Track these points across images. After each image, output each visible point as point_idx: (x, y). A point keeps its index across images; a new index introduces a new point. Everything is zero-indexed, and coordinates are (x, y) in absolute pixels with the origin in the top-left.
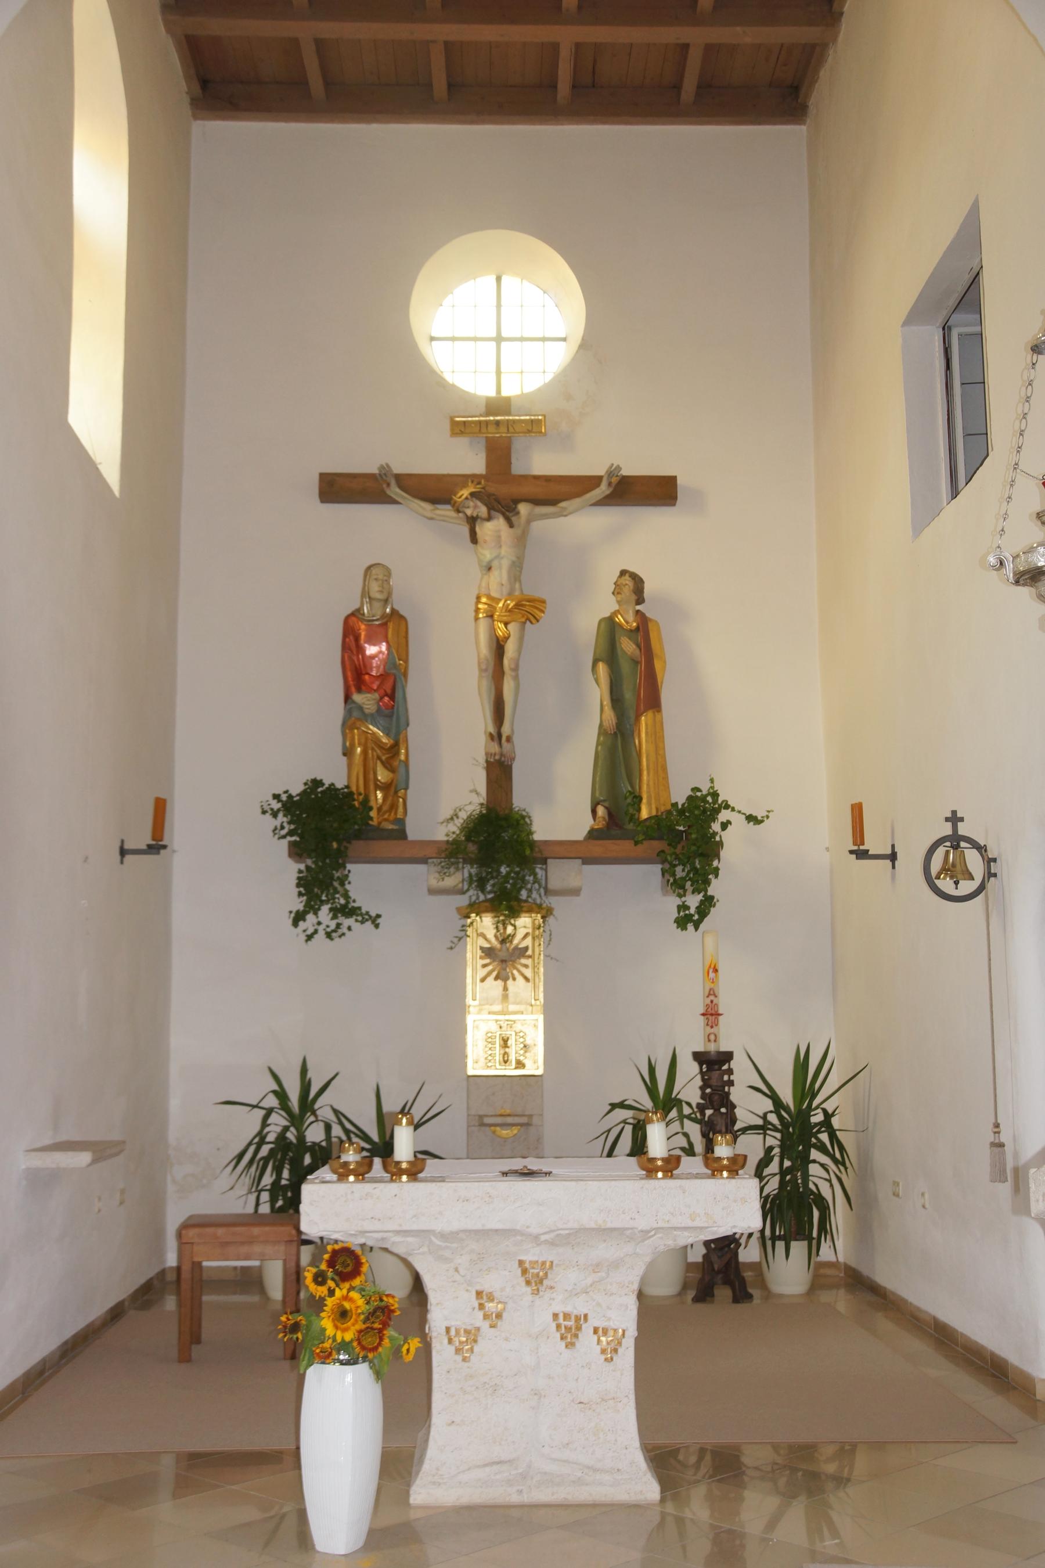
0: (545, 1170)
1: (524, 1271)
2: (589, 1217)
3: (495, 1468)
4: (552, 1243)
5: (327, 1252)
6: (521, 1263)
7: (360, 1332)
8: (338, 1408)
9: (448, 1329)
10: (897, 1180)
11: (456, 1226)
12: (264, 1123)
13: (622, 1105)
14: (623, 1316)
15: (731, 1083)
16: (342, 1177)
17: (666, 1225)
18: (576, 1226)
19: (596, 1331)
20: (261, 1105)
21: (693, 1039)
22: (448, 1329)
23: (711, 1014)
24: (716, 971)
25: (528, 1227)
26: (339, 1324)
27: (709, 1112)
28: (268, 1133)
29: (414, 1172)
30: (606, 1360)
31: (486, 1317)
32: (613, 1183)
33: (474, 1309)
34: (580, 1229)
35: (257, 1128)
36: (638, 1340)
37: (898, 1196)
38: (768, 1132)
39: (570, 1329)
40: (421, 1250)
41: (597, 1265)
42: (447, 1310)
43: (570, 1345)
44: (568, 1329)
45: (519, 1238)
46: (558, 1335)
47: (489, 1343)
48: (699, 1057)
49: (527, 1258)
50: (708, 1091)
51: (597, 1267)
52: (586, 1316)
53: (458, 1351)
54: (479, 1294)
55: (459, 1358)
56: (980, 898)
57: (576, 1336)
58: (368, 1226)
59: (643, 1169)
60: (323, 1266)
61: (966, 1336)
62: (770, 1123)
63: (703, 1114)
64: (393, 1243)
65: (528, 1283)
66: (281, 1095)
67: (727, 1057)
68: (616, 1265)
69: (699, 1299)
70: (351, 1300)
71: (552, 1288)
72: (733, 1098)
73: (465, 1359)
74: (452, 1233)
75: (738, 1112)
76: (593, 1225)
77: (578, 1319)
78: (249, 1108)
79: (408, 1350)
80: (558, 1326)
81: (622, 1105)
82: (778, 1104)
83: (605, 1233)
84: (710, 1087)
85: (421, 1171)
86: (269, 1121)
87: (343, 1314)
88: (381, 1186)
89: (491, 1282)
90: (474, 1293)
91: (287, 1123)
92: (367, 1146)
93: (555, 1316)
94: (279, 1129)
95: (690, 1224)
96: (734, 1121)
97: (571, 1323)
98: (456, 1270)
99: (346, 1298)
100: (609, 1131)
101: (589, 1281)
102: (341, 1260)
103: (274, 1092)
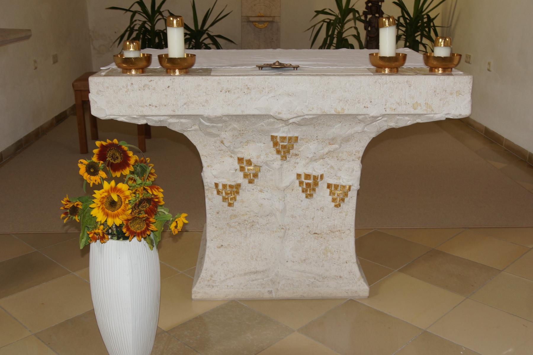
0: (294, 63)
1: (275, 144)
2: (330, 106)
3: (253, 276)
4: (299, 124)
5: (96, 147)
6: (273, 138)
7: (128, 220)
9: (216, 185)
10: (468, 54)
11: (219, 112)
13: (323, 12)
14: (350, 175)
16: (126, 71)
17: (393, 113)
18: (319, 112)
19: (329, 186)
20: (131, 9)
22: (216, 185)
25: (279, 113)
26: (110, 212)
27: (369, 16)
28: (136, 25)
29: (184, 66)
30: (336, 206)
31: (245, 176)
32: (351, 78)
33: (236, 170)
34: (322, 115)
36: (359, 192)
37: (469, 63)
38: (400, 28)
39: (309, 185)
40: (193, 128)
41: (333, 139)
42: (216, 169)
43: (309, 196)
44: (308, 185)
45: (272, 120)
46: (300, 189)
49: (279, 134)
50: (370, 4)
51: (332, 141)
52: (322, 176)
53: (224, 199)
54: (240, 160)
55: (226, 204)
57: (314, 190)
58: (147, 111)
59: (374, 65)
60: (95, 159)
61: (509, 141)
62: (401, 23)
63: (366, 17)
64: (170, 124)
65: (278, 152)
68: (347, 139)
70: (120, 191)
71: (296, 155)
72: (383, 9)
73: (230, 205)
74: (217, 117)
76: (333, 112)
77: (315, 178)
78: (124, 11)
79: (176, 227)
80: (301, 183)
81: (323, 12)
83: (340, 117)
84: (371, 2)
85: (192, 65)
86: (135, 19)
88: (156, 79)
89: (250, 152)
90: (236, 159)
91: (145, 20)
92: (188, 32)
93: (299, 176)
94: (141, 23)
95: (412, 111)
97: (311, 181)
98: (222, 142)
99: (114, 189)
100: (315, 26)
101: (326, 150)
102: (109, 154)
103: (137, 2)
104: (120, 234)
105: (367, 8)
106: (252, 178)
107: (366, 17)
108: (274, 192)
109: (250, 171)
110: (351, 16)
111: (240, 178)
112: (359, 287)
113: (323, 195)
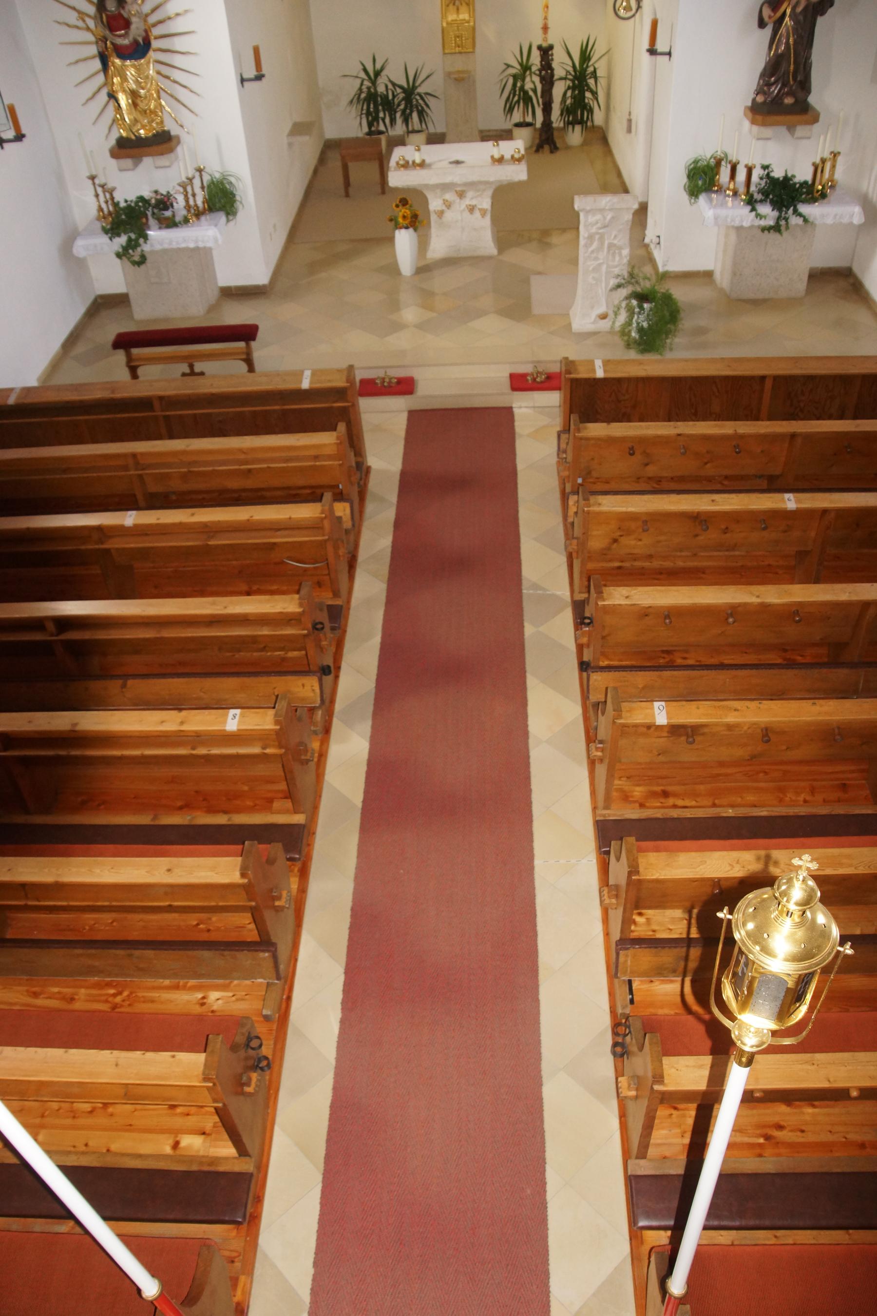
8: (404, 241)
12: (362, 84)
15: (552, 60)
21: (538, 39)
23: (545, 29)
24: (547, 7)
35: (358, 86)
39: (471, 209)
47: (449, 216)
48: (540, 48)
56: (633, 19)
67: (551, 47)
69: (537, 151)
75: (556, 72)
82: (574, 66)
87: (404, 217)
96: (552, 75)
104: (407, 228)
105: (541, 65)
107: (540, 73)
109: (448, 205)
110: (528, 73)
111: (444, 208)
112: (494, 251)
113: (477, 214)
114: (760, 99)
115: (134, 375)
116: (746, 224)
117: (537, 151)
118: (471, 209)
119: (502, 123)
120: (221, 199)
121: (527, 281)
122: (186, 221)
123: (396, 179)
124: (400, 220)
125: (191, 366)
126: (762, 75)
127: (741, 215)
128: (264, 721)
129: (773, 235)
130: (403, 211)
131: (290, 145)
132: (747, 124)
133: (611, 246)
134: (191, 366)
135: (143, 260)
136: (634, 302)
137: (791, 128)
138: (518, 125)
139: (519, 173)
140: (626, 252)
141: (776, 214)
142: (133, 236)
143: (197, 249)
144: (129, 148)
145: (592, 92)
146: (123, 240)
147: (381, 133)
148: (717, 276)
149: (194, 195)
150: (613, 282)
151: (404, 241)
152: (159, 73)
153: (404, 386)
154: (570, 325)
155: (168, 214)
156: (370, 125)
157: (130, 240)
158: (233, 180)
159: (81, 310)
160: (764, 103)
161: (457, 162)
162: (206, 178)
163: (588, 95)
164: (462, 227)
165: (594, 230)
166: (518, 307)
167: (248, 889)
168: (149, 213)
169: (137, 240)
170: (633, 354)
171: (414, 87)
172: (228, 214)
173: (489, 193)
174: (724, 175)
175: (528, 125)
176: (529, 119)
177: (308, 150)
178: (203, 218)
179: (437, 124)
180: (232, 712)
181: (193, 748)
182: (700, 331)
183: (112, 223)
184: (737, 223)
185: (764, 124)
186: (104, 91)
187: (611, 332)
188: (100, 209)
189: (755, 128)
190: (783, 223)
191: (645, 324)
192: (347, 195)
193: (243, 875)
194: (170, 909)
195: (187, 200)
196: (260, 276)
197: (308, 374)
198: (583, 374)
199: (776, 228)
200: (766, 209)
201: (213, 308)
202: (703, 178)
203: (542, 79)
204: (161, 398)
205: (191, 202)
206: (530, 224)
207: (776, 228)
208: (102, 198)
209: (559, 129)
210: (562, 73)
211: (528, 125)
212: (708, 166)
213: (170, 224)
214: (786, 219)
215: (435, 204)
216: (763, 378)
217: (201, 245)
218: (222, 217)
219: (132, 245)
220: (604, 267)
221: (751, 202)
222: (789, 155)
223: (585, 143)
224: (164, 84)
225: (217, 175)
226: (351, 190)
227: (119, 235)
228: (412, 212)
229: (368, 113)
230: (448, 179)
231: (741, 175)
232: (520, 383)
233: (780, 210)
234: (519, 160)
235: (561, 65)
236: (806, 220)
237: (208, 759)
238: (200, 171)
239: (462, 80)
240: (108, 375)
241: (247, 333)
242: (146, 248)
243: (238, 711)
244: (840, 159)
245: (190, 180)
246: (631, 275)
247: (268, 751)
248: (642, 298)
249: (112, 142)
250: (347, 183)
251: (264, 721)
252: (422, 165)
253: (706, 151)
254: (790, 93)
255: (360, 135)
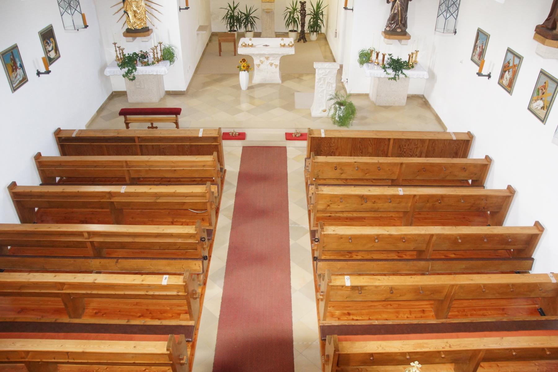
48: (300, 2)
66: (230, 6)
67: (305, 2)
69: (298, 41)
106: (262, 63)
108: (265, 66)
109: (262, 62)
112: (280, 82)
113: (274, 66)
114: (388, 29)
115: (128, 127)
116: (382, 76)
117: (298, 41)
118: (271, 64)
119: (285, 30)
120: (168, 55)
121: (293, 94)
122: (153, 63)
123: (241, 51)
124: (242, 67)
125: (152, 124)
126: (389, 20)
127: (380, 72)
128: (179, 281)
129: (393, 81)
130: (243, 64)
131: (198, 34)
132: (383, 38)
133: (328, 83)
134: (152, 124)
135: (134, 79)
136: (337, 106)
137: (400, 40)
138: (290, 31)
139: (291, 51)
140: (334, 85)
141: (394, 73)
142: (130, 69)
143: (157, 75)
144: (131, 33)
145: (321, 20)
146: (126, 70)
147: (235, 31)
148: (370, 96)
149: (157, 53)
150: (329, 97)
151: (243, 76)
152: (146, 4)
153: (241, 136)
154: (310, 114)
155: (146, 60)
156: (231, 28)
157: (129, 70)
158: (173, 48)
159: (106, 97)
160: (389, 30)
161: (266, 46)
162: (163, 47)
163: (319, 21)
164: (267, 71)
165: (321, 76)
166: (290, 106)
167: (170, 356)
168: (138, 60)
169: (132, 70)
170: (336, 127)
171: (249, 14)
172: (171, 62)
173: (279, 58)
174: (374, 56)
175: (295, 31)
176: (295, 29)
177: (205, 36)
178: (160, 63)
179: (258, 29)
180: (165, 276)
181: (147, 292)
182: (364, 118)
183: (122, 62)
184: (379, 76)
185: (389, 39)
186: (123, 10)
187: (328, 117)
188: (117, 57)
189: (386, 40)
190: (397, 76)
191: (341, 115)
192: (220, 55)
193: (168, 350)
194: (134, 364)
195: (154, 55)
196: (182, 87)
197: (201, 130)
198: (316, 135)
199: (394, 78)
200: (390, 71)
201: (161, 100)
202: (365, 58)
203: (301, 14)
204: (139, 137)
205: (156, 56)
206: (294, 72)
207: (394, 78)
208: (118, 52)
209: (307, 33)
210: (310, 13)
211: (295, 31)
212: (367, 53)
213: (147, 64)
214: (398, 75)
215: (256, 61)
216: (389, 139)
217: (159, 74)
218: (168, 62)
219: (129, 72)
220: (325, 91)
221: (384, 68)
222: (399, 50)
223: (318, 40)
224: (148, 9)
225: (167, 46)
226: (221, 53)
227: (124, 68)
228: (247, 64)
229: (230, 23)
230: (262, 52)
231: (381, 57)
232: (289, 137)
233: (396, 72)
234: (291, 46)
235: (309, 9)
236: (406, 76)
237: (153, 297)
238: (160, 44)
239: (269, 12)
240: (116, 126)
241: (176, 112)
242: (135, 73)
243: (167, 276)
244: (418, 53)
245: (156, 47)
246: (336, 95)
247: (180, 294)
248: (341, 104)
249: (124, 30)
250: (220, 50)
251: (179, 281)
252: (252, 46)
253: (367, 48)
254: (399, 28)
255: (227, 31)
